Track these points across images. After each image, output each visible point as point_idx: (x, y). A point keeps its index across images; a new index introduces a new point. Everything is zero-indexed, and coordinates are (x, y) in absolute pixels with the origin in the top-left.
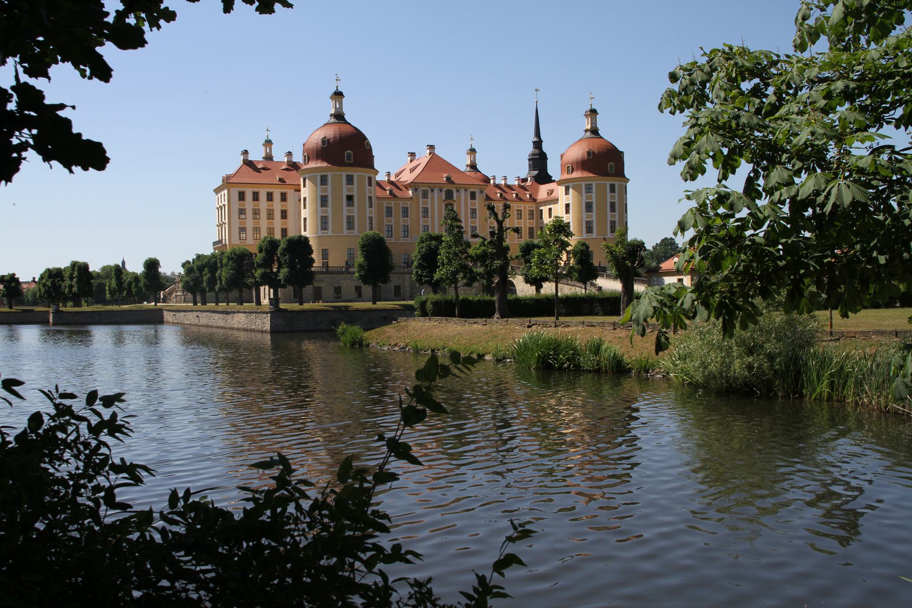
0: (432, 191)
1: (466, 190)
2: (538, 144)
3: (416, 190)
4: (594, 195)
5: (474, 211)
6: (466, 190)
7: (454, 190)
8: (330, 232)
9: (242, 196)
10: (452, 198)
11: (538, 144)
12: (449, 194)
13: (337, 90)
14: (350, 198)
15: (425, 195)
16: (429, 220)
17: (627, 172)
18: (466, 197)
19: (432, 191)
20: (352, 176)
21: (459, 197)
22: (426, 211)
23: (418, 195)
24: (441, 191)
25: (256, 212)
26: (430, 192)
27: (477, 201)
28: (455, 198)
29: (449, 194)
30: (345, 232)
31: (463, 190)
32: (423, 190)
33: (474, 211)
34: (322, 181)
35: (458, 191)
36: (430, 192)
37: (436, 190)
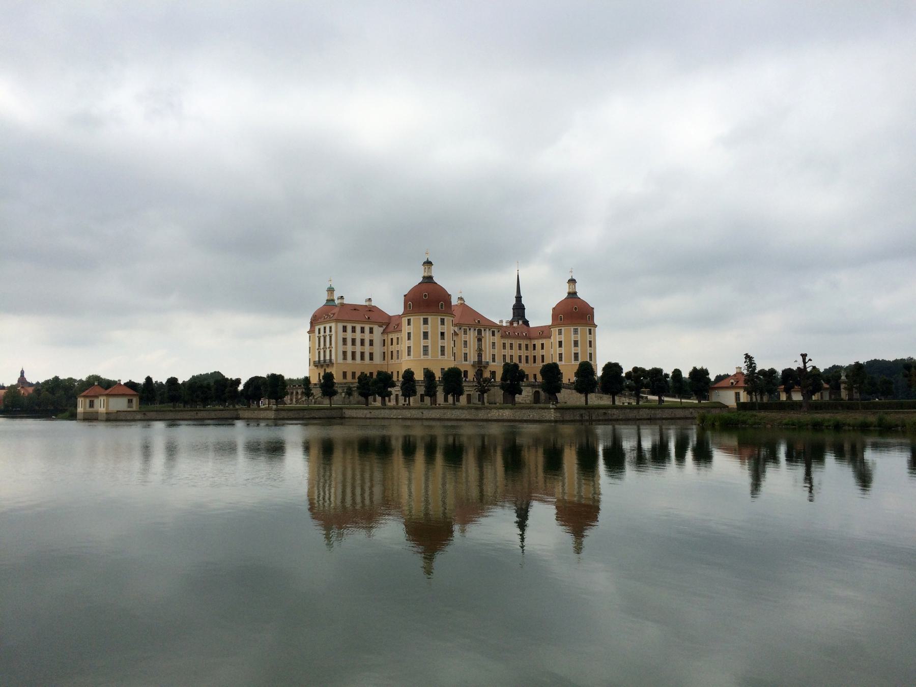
0: (470, 329)
1: (490, 330)
2: (519, 298)
3: (460, 329)
4: (579, 336)
5: (494, 344)
6: (490, 330)
7: (483, 329)
8: (429, 357)
9: (345, 329)
10: (481, 334)
11: (519, 298)
12: (480, 332)
13: (428, 260)
14: (442, 334)
15: (465, 333)
16: (468, 349)
17: (596, 322)
18: (489, 334)
19: (470, 329)
20: (444, 319)
21: (485, 334)
22: (465, 342)
23: (461, 332)
24: (475, 330)
25: (354, 341)
26: (468, 330)
27: (496, 337)
28: (483, 335)
29: (480, 332)
30: (440, 357)
31: (487, 330)
32: (464, 329)
33: (494, 344)
34: (441, 322)
35: (485, 330)
36: (468, 330)
37: (472, 329)
